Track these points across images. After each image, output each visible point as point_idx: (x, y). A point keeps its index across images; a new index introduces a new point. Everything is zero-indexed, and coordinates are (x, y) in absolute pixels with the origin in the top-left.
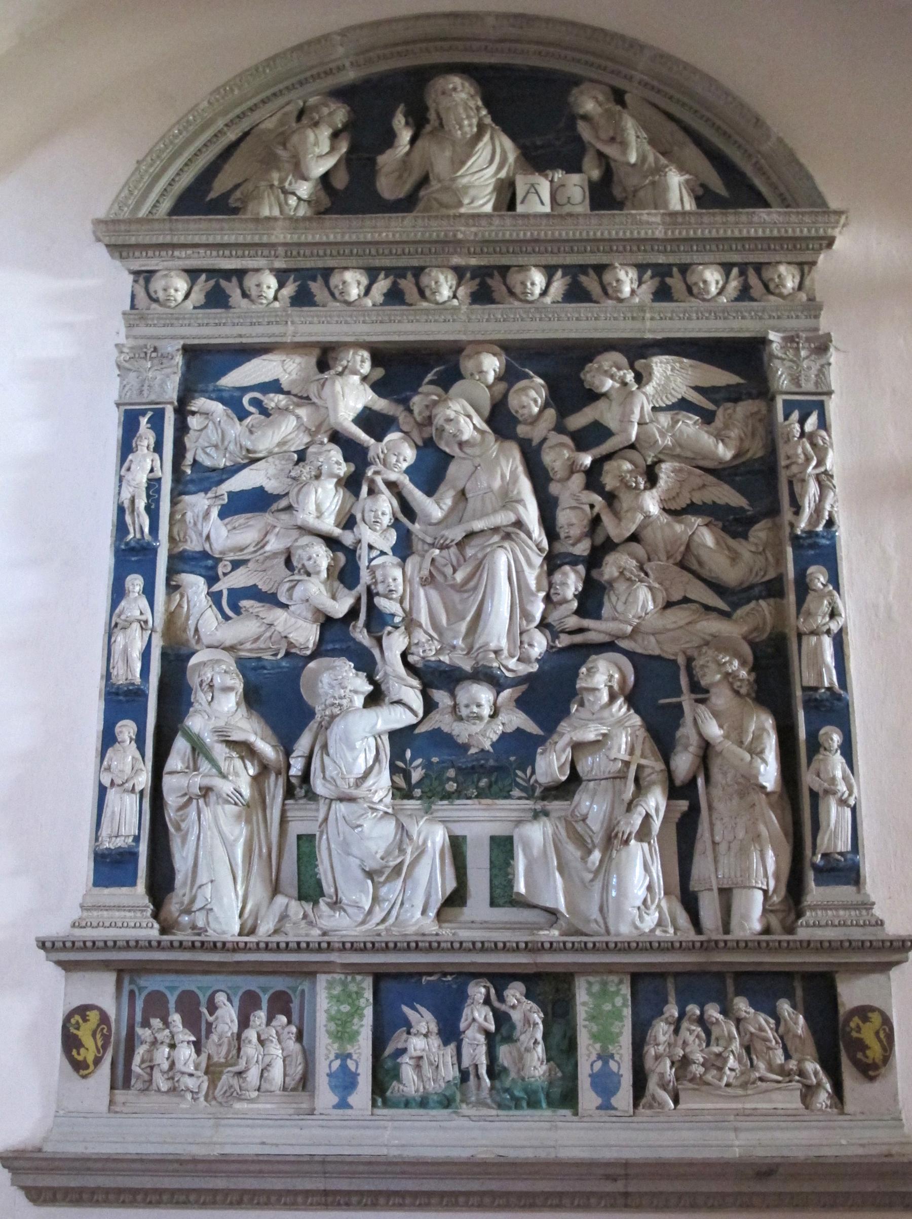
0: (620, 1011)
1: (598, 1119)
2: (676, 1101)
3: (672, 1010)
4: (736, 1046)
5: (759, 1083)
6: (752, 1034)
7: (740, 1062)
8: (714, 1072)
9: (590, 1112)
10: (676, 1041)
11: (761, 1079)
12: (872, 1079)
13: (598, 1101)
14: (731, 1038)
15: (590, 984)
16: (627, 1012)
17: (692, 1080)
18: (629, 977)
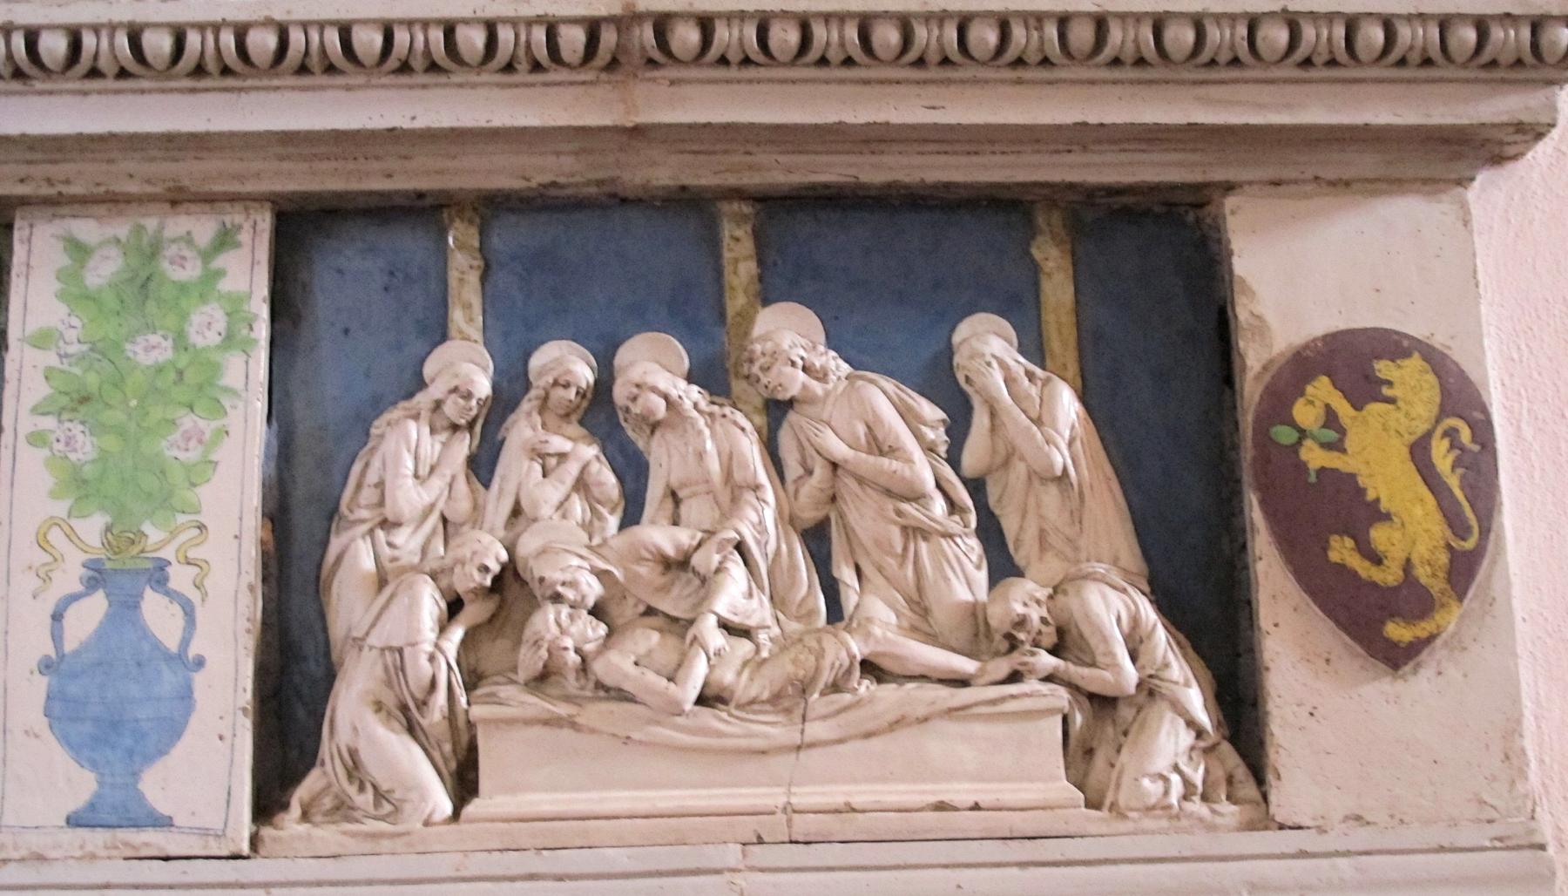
0: (215, 369)
1: (78, 874)
2: (464, 782)
3: (463, 366)
4: (760, 520)
5: (866, 687)
6: (835, 466)
7: (777, 601)
8: (648, 639)
9: (35, 841)
10: (477, 507)
11: (871, 668)
12: (1397, 658)
13: (80, 786)
14: (736, 490)
15: (79, 251)
16: (249, 371)
17: (543, 678)
18: (265, 221)
